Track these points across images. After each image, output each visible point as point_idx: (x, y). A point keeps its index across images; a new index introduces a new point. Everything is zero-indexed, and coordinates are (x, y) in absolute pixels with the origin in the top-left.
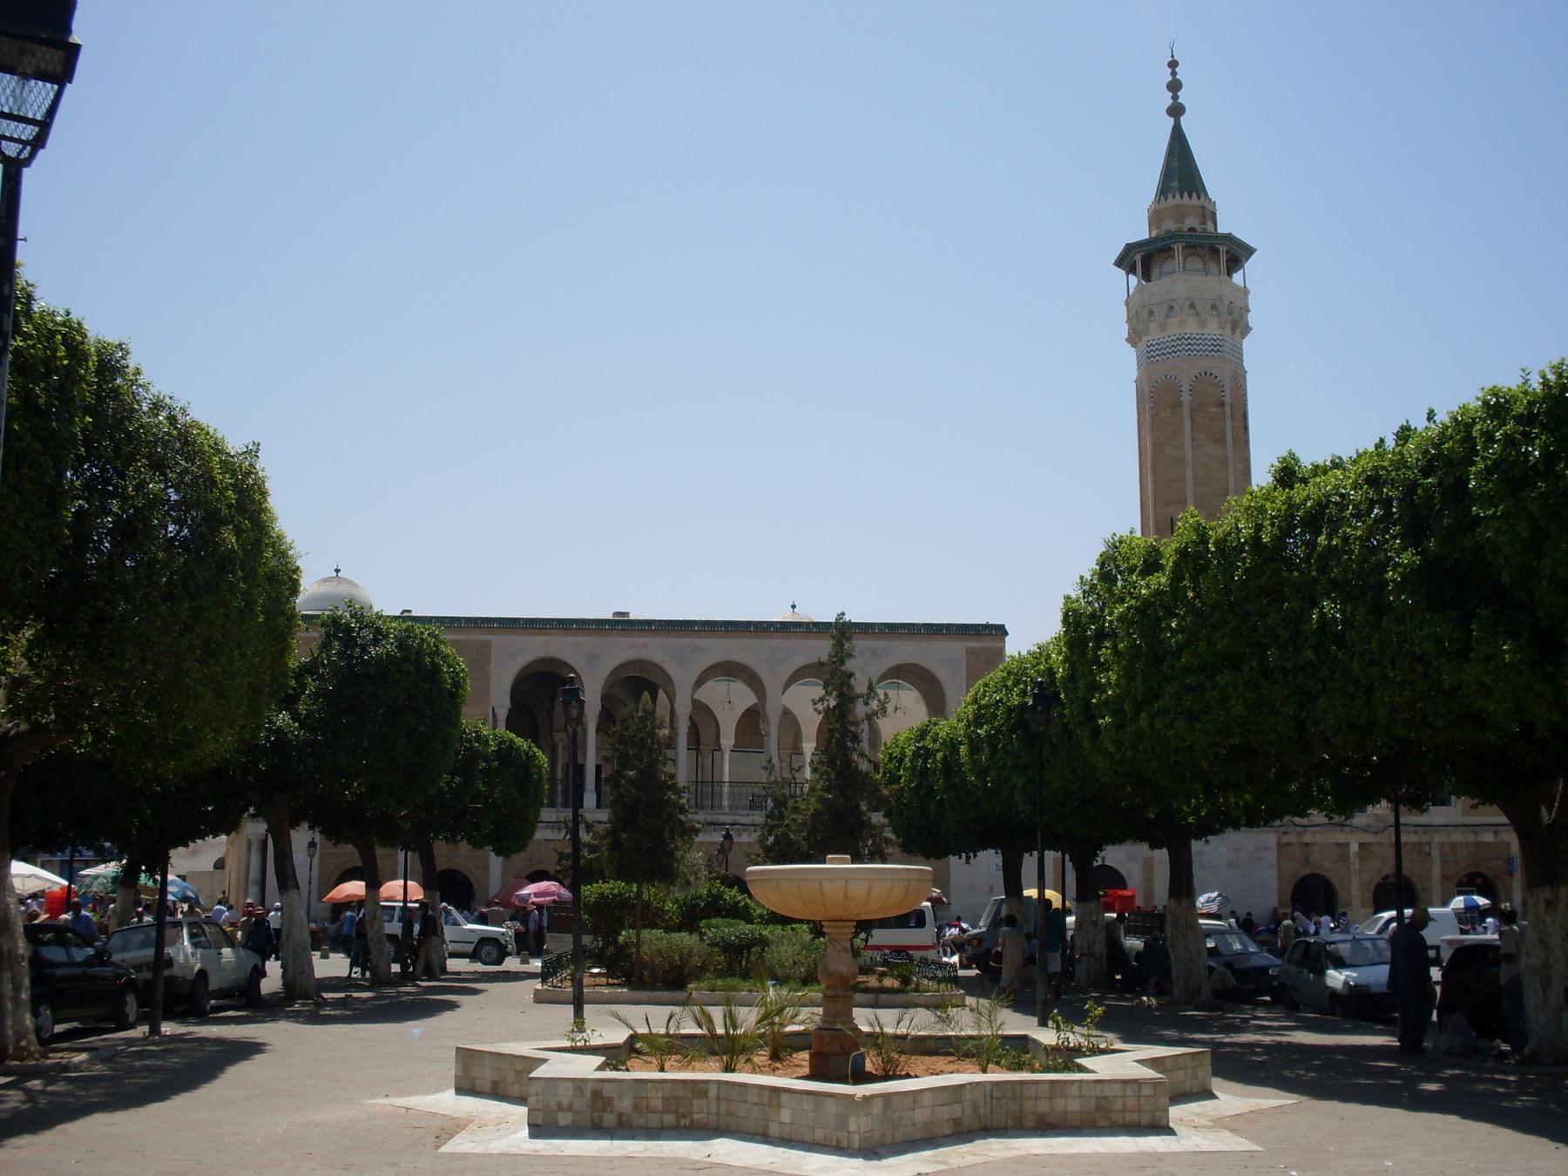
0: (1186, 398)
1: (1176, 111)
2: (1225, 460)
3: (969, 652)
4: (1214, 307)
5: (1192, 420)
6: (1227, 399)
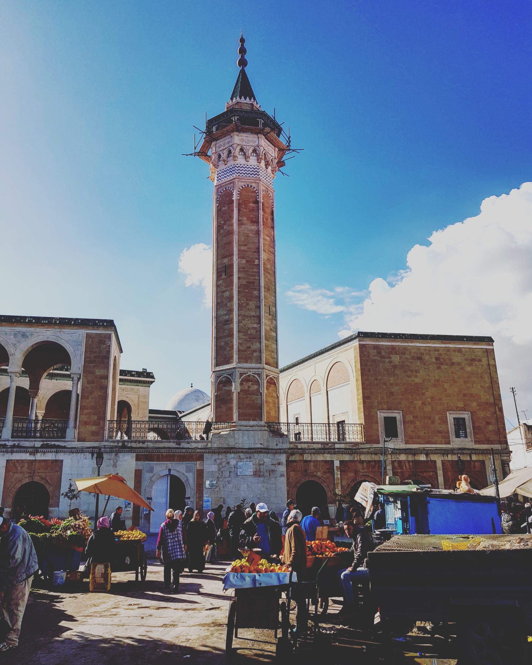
1: (243, 63)
2: (258, 233)
3: (88, 336)
4: (254, 151)
5: (239, 210)
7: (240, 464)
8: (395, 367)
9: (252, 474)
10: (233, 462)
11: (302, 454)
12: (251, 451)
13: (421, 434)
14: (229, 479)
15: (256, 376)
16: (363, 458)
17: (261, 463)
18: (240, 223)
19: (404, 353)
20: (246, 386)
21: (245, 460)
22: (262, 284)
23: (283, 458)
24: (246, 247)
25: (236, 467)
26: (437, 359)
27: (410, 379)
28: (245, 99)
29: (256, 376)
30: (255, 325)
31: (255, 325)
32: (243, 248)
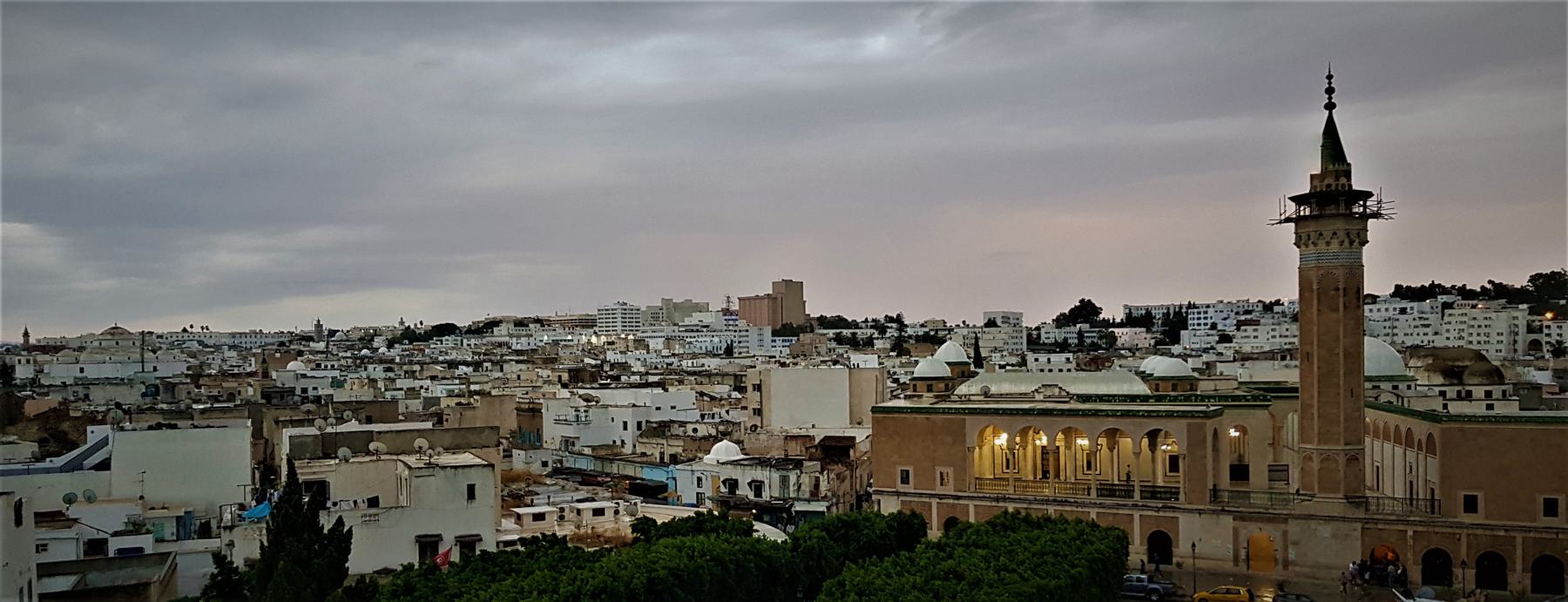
6: (1341, 286)
12: (1330, 518)
23: (1359, 526)
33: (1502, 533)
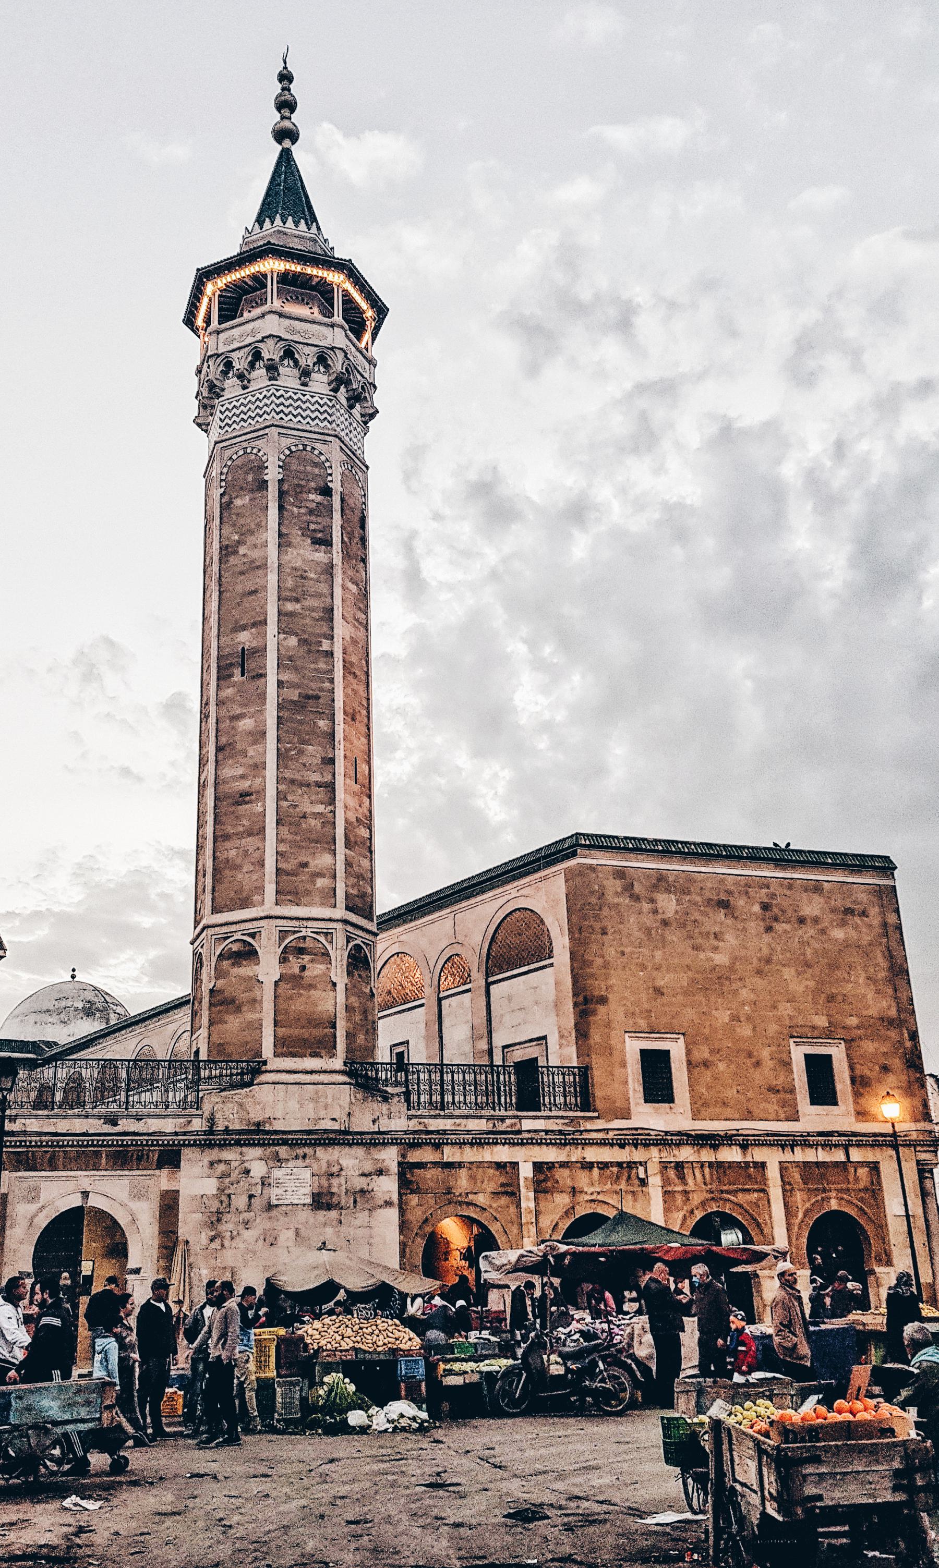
0: (273, 474)
5: (281, 508)
7: (278, 1173)
8: (665, 923)
9: (309, 1200)
10: (258, 1169)
11: (437, 1146)
13: (731, 1093)
14: (246, 1216)
15: (322, 938)
16: (592, 1154)
17: (335, 1169)
18: (284, 541)
19: (686, 891)
20: (294, 966)
21: (291, 1164)
22: (339, 704)
23: (390, 1156)
24: (298, 606)
25: (265, 1182)
26: (766, 907)
27: (702, 956)
28: (297, 224)
29: (322, 938)
30: (320, 808)
31: (320, 808)
32: (289, 607)
33: (731, 1155)
